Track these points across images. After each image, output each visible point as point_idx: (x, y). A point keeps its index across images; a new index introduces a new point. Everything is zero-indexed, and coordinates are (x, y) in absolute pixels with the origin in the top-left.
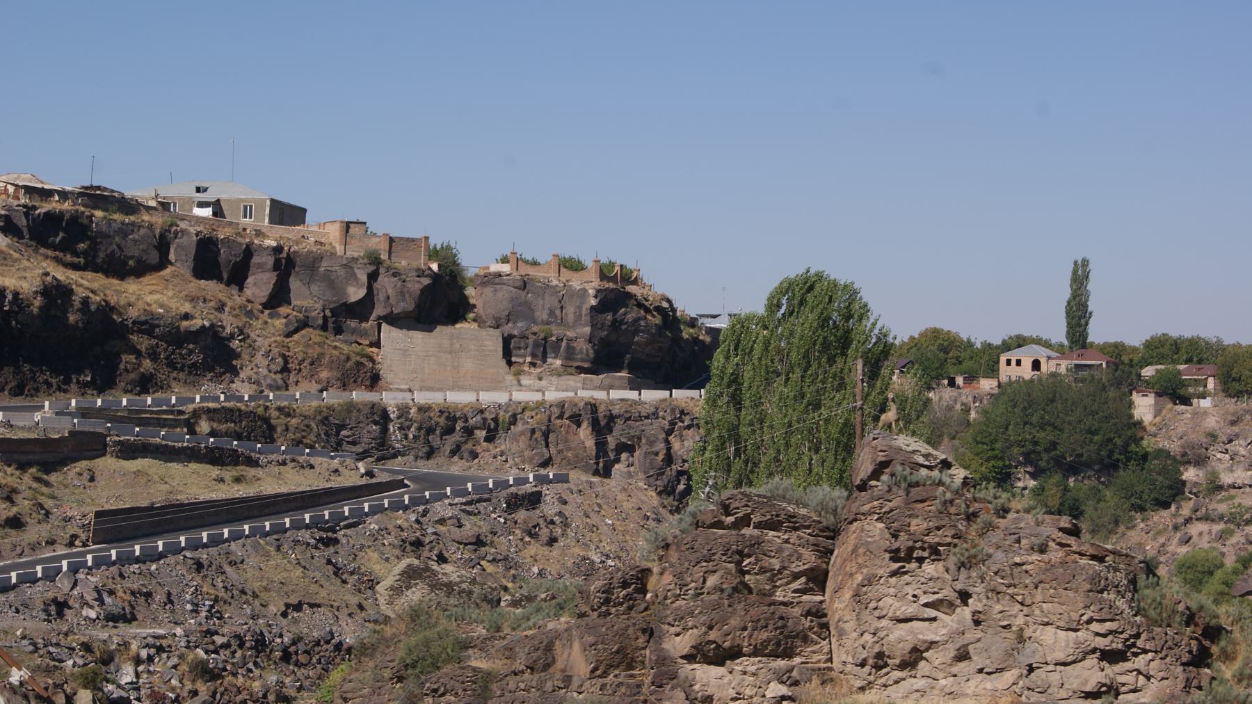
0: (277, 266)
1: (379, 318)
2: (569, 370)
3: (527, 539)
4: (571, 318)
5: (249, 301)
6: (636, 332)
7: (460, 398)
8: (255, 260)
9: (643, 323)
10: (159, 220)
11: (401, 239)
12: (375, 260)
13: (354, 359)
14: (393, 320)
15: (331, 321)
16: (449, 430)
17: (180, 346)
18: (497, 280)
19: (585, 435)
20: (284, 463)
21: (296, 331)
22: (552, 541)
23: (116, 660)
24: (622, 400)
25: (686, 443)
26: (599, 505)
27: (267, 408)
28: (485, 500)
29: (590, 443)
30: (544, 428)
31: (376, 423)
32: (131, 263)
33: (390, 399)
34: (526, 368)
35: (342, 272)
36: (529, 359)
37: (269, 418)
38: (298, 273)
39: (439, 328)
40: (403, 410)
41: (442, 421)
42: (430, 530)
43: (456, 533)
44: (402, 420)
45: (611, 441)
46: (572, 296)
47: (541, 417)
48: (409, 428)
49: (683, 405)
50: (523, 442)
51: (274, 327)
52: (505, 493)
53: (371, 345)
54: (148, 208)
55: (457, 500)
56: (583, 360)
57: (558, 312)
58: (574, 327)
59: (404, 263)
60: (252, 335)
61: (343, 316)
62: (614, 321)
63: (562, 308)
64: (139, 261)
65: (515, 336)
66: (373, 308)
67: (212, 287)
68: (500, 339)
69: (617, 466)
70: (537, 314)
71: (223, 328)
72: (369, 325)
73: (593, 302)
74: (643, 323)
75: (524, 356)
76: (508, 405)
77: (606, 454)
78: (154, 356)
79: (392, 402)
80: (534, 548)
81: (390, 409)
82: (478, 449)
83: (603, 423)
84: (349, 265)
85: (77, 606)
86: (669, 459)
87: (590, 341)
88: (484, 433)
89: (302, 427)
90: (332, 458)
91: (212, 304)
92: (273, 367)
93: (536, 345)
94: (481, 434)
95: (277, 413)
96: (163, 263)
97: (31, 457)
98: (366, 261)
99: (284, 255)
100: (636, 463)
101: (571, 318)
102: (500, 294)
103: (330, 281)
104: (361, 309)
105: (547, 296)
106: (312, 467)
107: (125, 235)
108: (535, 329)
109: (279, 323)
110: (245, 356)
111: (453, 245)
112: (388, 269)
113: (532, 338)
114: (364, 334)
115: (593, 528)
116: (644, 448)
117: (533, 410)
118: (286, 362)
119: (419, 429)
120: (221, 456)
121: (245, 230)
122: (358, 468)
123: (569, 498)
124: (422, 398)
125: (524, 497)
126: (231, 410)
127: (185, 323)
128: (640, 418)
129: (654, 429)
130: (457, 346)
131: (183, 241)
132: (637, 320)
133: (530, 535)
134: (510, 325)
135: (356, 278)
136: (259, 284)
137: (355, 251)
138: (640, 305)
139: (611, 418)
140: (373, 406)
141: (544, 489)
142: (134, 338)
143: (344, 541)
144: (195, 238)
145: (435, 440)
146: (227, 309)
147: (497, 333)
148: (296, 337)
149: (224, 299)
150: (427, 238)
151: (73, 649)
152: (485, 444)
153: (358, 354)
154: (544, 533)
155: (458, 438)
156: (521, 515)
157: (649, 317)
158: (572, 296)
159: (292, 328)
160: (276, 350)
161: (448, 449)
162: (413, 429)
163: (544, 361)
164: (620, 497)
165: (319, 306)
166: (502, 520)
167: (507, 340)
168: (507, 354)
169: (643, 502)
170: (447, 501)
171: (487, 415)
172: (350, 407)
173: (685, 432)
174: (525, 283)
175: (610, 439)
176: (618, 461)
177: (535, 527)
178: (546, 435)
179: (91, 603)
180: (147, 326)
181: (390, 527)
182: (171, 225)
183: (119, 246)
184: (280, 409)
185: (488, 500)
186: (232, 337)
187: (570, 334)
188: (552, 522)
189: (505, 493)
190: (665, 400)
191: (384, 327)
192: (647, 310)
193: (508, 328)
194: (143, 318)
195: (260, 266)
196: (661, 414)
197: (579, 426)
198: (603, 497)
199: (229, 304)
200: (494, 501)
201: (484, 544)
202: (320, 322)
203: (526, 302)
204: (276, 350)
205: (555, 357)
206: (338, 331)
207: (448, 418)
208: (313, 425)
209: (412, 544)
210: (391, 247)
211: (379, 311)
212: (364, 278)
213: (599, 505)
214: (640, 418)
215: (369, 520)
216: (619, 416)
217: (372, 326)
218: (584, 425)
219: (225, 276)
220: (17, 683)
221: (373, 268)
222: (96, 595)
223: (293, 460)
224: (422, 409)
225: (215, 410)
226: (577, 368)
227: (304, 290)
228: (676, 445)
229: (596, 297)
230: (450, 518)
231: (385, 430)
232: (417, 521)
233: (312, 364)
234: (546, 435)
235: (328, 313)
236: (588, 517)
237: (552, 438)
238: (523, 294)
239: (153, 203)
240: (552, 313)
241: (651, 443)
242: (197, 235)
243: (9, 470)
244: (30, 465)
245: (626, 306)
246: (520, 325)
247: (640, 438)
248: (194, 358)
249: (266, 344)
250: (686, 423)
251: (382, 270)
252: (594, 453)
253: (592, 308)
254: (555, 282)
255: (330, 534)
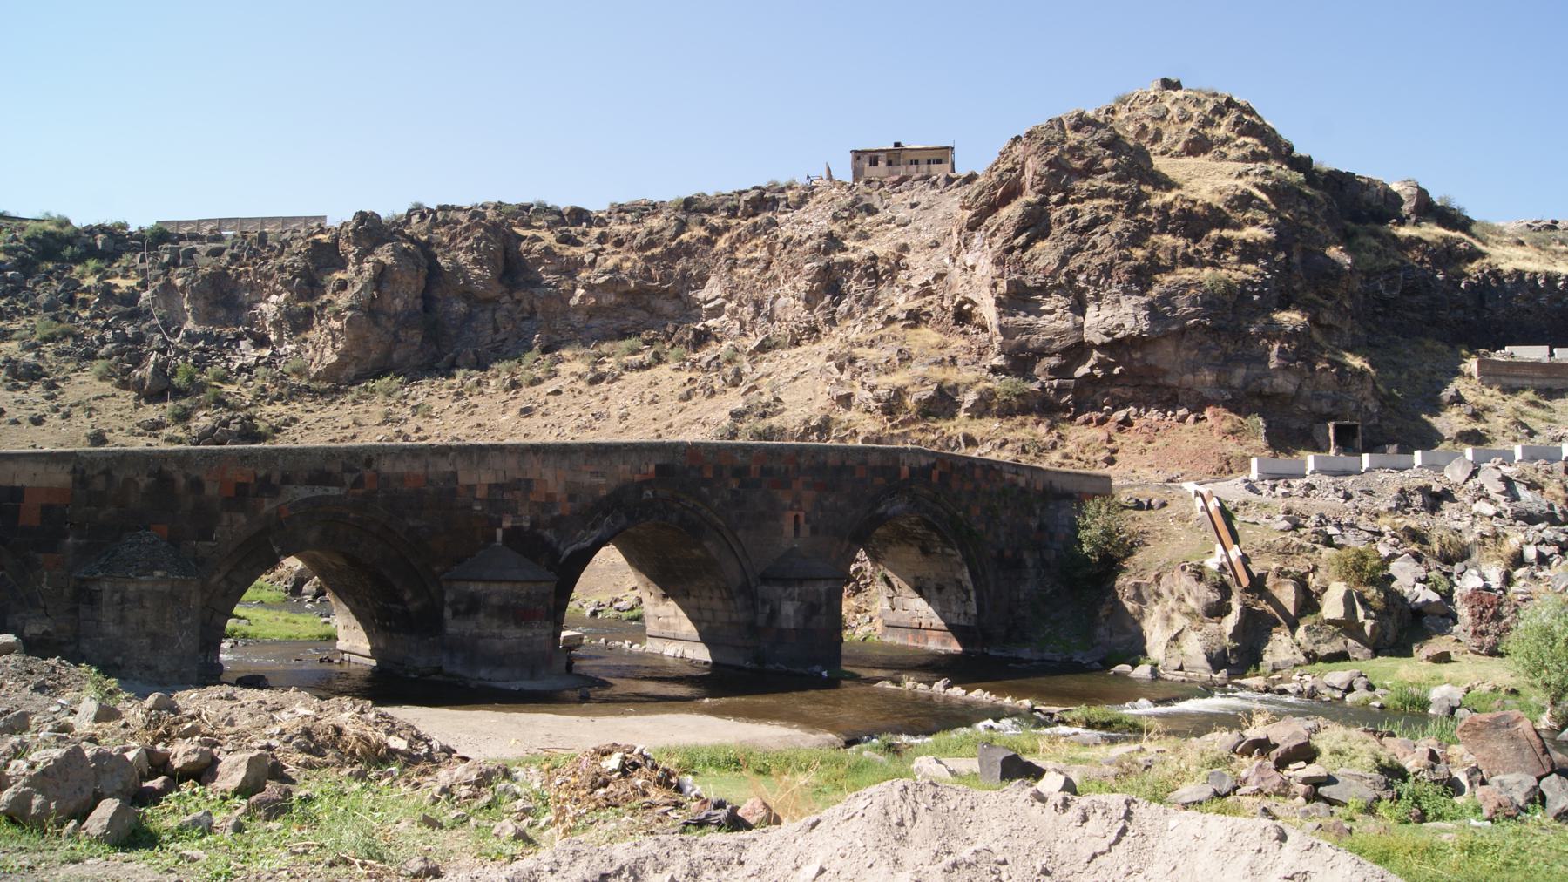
23: (1475, 558)
85: (1466, 499)
97: (1527, 382)
151: (1381, 534)
179: (1493, 496)
220: (1215, 567)
222: (1502, 487)
243: (1488, 392)
244: (1524, 389)
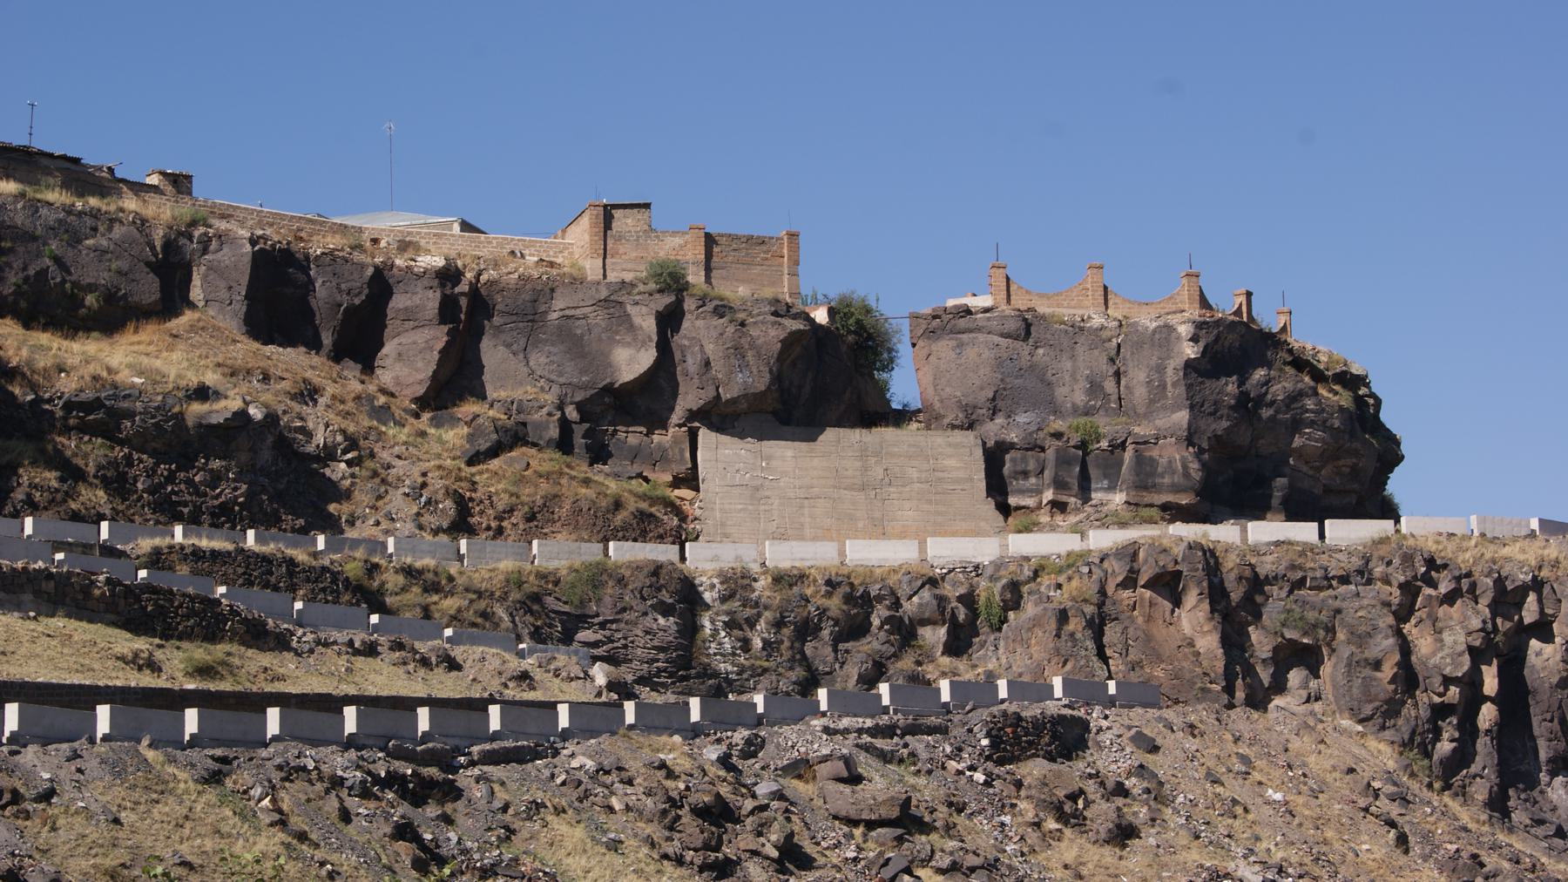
0: (448, 310)
1: (693, 415)
2: (1146, 512)
3: (1051, 824)
4: (1140, 394)
5: (383, 391)
6: (1296, 425)
7: (876, 554)
8: (398, 302)
9: (1310, 404)
10: (163, 212)
11: (734, 238)
12: (672, 281)
13: (632, 505)
14: (721, 417)
15: (579, 431)
16: (855, 629)
17: (187, 462)
18: (963, 323)
19: (1193, 621)
20: (371, 650)
21: (495, 452)
22: (1124, 834)
24: (1278, 544)
25: (1447, 637)
26: (1244, 759)
27: (373, 569)
28: (931, 731)
29: (1209, 643)
30: (1089, 610)
31: (666, 610)
32: (90, 300)
33: (704, 560)
34: (1044, 518)
35: (598, 318)
36: (1048, 495)
37: (381, 591)
38: (499, 330)
39: (830, 434)
40: (736, 584)
41: (835, 604)
42: (763, 789)
43: (843, 798)
44: (735, 604)
45: (1261, 642)
46: (1139, 345)
47: (1078, 586)
48: (752, 623)
49: (1433, 548)
50: (1041, 644)
51: (440, 440)
52: (984, 714)
53: (677, 483)
54: (139, 188)
55: (845, 722)
56: (1176, 489)
57: (1109, 385)
58: (1148, 415)
59: (743, 291)
60: (385, 456)
61: (610, 416)
62: (1243, 399)
63: (1118, 375)
64: (110, 297)
65: (1012, 446)
66: (675, 394)
67: (293, 361)
68: (979, 452)
69: (1278, 701)
70: (1061, 392)
71: (309, 435)
72: (669, 438)
73: (1191, 351)
74: (1310, 404)
75: (1039, 492)
76: (999, 565)
77: (1249, 671)
78: (117, 484)
79: (710, 567)
80: (1071, 847)
81: (703, 581)
82: (930, 671)
83: (1236, 596)
84: (613, 302)
86: (1408, 678)
87: (1190, 441)
88: (942, 632)
89: (470, 615)
90: (521, 655)
91: (285, 385)
92: (430, 519)
93: (1063, 460)
94: (935, 636)
95: (401, 579)
96: (173, 300)
98: (652, 286)
99: (463, 287)
100: (1328, 693)
101: (1140, 394)
102: (970, 353)
103: (572, 339)
104: (646, 400)
105: (1080, 349)
106: (453, 665)
107: (75, 240)
108: (1059, 425)
109: (455, 436)
110: (362, 497)
111: (873, 305)
112: (703, 300)
113: (1052, 446)
114: (659, 459)
115: (1233, 808)
116: (1345, 652)
117: (1060, 571)
118: (463, 507)
119: (779, 624)
120: (161, 612)
121: (375, 241)
122: (587, 676)
123: (1165, 740)
124: (784, 555)
125: (1038, 725)
126: (266, 559)
127: (197, 408)
128: (1327, 581)
129: (1365, 606)
130: (878, 472)
131: (225, 256)
132: (1295, 397)
133: (1062, 817)
134: (999, 420)
135: (632, 328)
136: (408, 358)
137: (628, 265)
138: (1300, 363)
139: (1257, 584)
140: (657, 570)
141: (1095, 716)
142: (69, 444)
143: (478, 792)
144: (248, 248)
145: (819, 650)
146: (322, 401)
147: (969, 438)
148: (495, 464)
149: (316, 381)
150: (793, 236)
152: (946, 661)
153: (643, 497)
154: (1102, 812)
155: (876, 645)
156: (1034, 769)
157: (1323, 392)
158: (1139, 345)
159: (484, 445)
160: (437, 483)
161: (851, 673)
162: (761, 625)
163: (1086, 499)
164: (1295, 744)
165: (550, 398)
166: (979, 777)
167: (994, 457)
168: (997, 488)
169: (1358, 759)
170: (817, 723)
171: (951, 591)
172: (598, 575)
173: (1443, 611)
174: (1028, 326)
175: (1255, 634)
176: (1279, 686)
177: (1073, 797)
178: (1097, 627)
180: (102, 413)
181: (634, 766)
182: (193, 223)
183: (57, 260)
184: (409, 572)
185: (942, 730)
186: (328, 454)
187: (1142, 430)
188: (1121, 790)
189: (984, 714)
190: (1384, 541)
191: (705, 436)
192: (1319, 376)
193: (995, 429)
194: (89, 395)
195: (409, 315)
196: (1379, 570)
197: (1177, 603)
198: (1253, 742)
199: (330, 389)
200: (957, 732)
201: (926, 828)
202: (554, 432)
203: (1032, 367)
204: (437, 483)
205: (1111, 488)
206: (599, 454)
207: (849, 599)
208: (501, 612)
209: (701, 812)
210: (709, 255)
211: (689, 398)
212: (649, 325)
213: (1244, 759)
214: (1327, 581)
215: (570, 747)
216: (1273, 580)
217: (676, 441)
218: (1191, 598)
219: (327, 339)
221: (669, 299)
223: (398, 646)
224: (781, 579)
225: (215, 555)
226: (1165, 507)
227: (516, 365)
228: (1423, 644)
229: (1194, 339)
230: (825, 759)
231: (690, 629)
232: (724, 761)
233: (531, 517)
234: (1097, 627)
235: (572, 413)
236: (1215, 782)
237: (1111, 634)
238: (1024, 349)
239: (154, 180)
240: (1095, 388)
241: (1360, 638)
242: (253, 241)
245: (1269, 365)
246: (1022, 418)
247: (1331, 630)
248: (225, 492)
249: (416, 471)
250: (1444, 588)
251: (689, 304)
252: (1220, 665)
253: (1189, 365)
254: (1097, 320)
255: (432, 771)
